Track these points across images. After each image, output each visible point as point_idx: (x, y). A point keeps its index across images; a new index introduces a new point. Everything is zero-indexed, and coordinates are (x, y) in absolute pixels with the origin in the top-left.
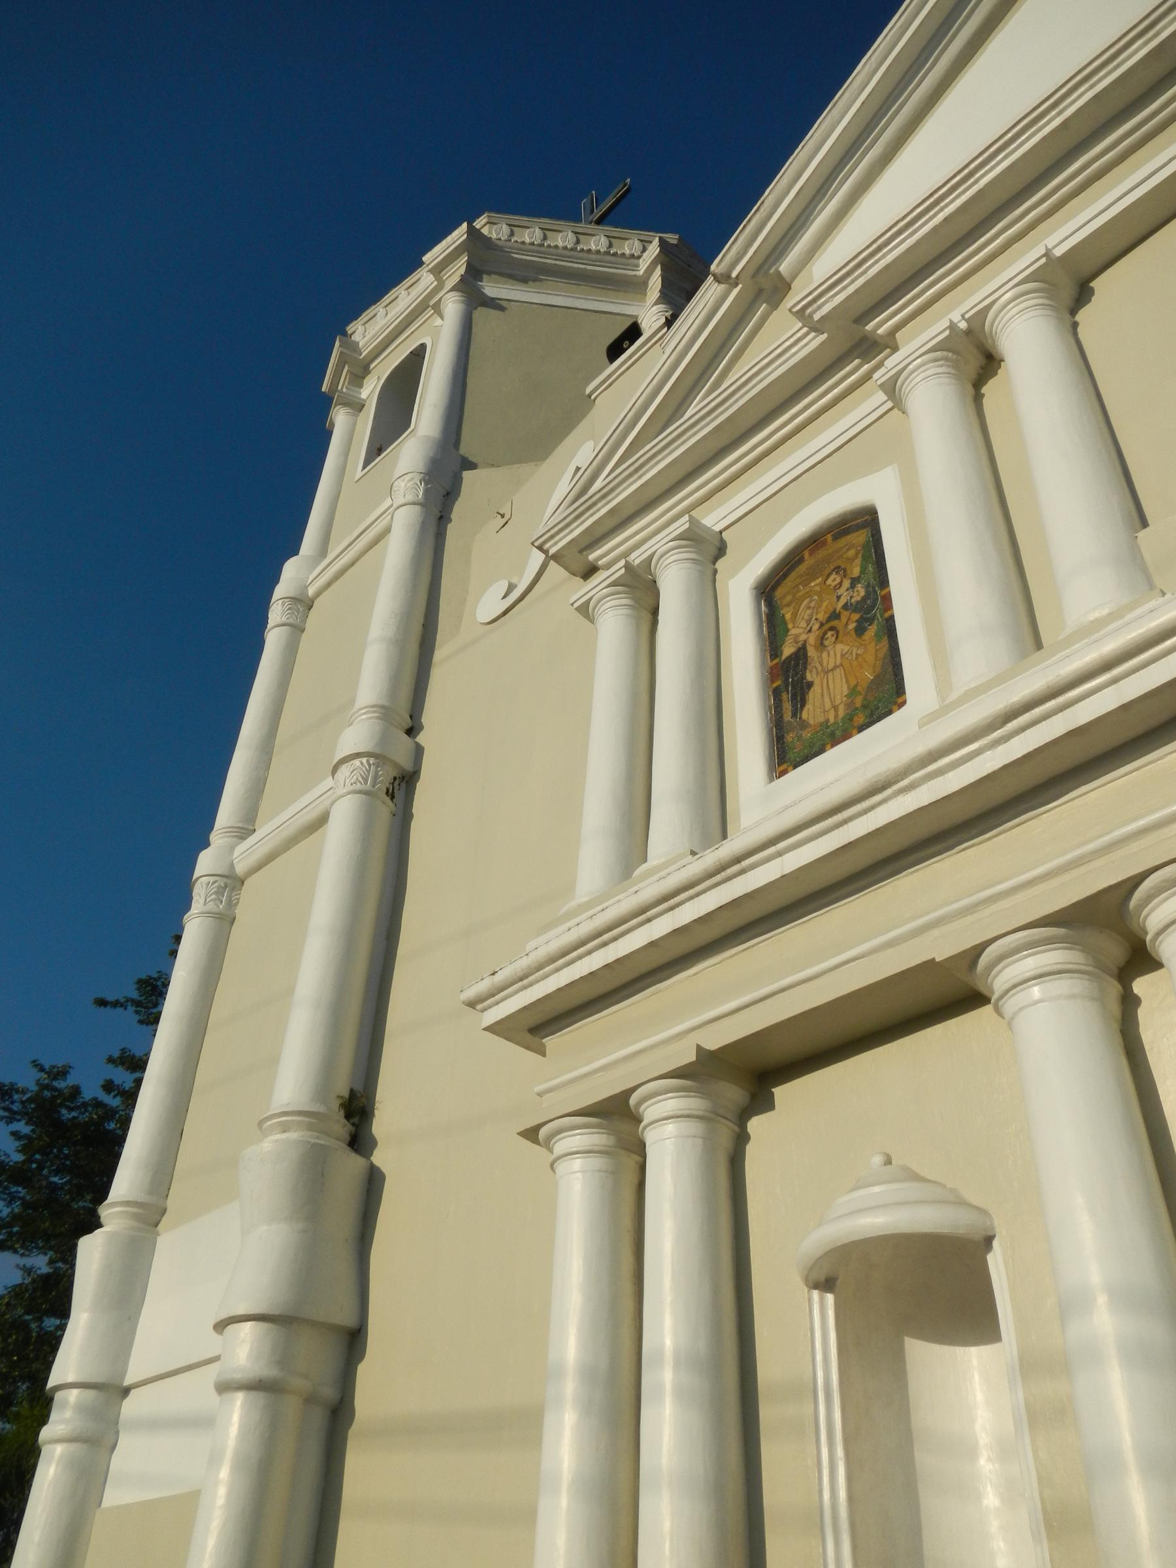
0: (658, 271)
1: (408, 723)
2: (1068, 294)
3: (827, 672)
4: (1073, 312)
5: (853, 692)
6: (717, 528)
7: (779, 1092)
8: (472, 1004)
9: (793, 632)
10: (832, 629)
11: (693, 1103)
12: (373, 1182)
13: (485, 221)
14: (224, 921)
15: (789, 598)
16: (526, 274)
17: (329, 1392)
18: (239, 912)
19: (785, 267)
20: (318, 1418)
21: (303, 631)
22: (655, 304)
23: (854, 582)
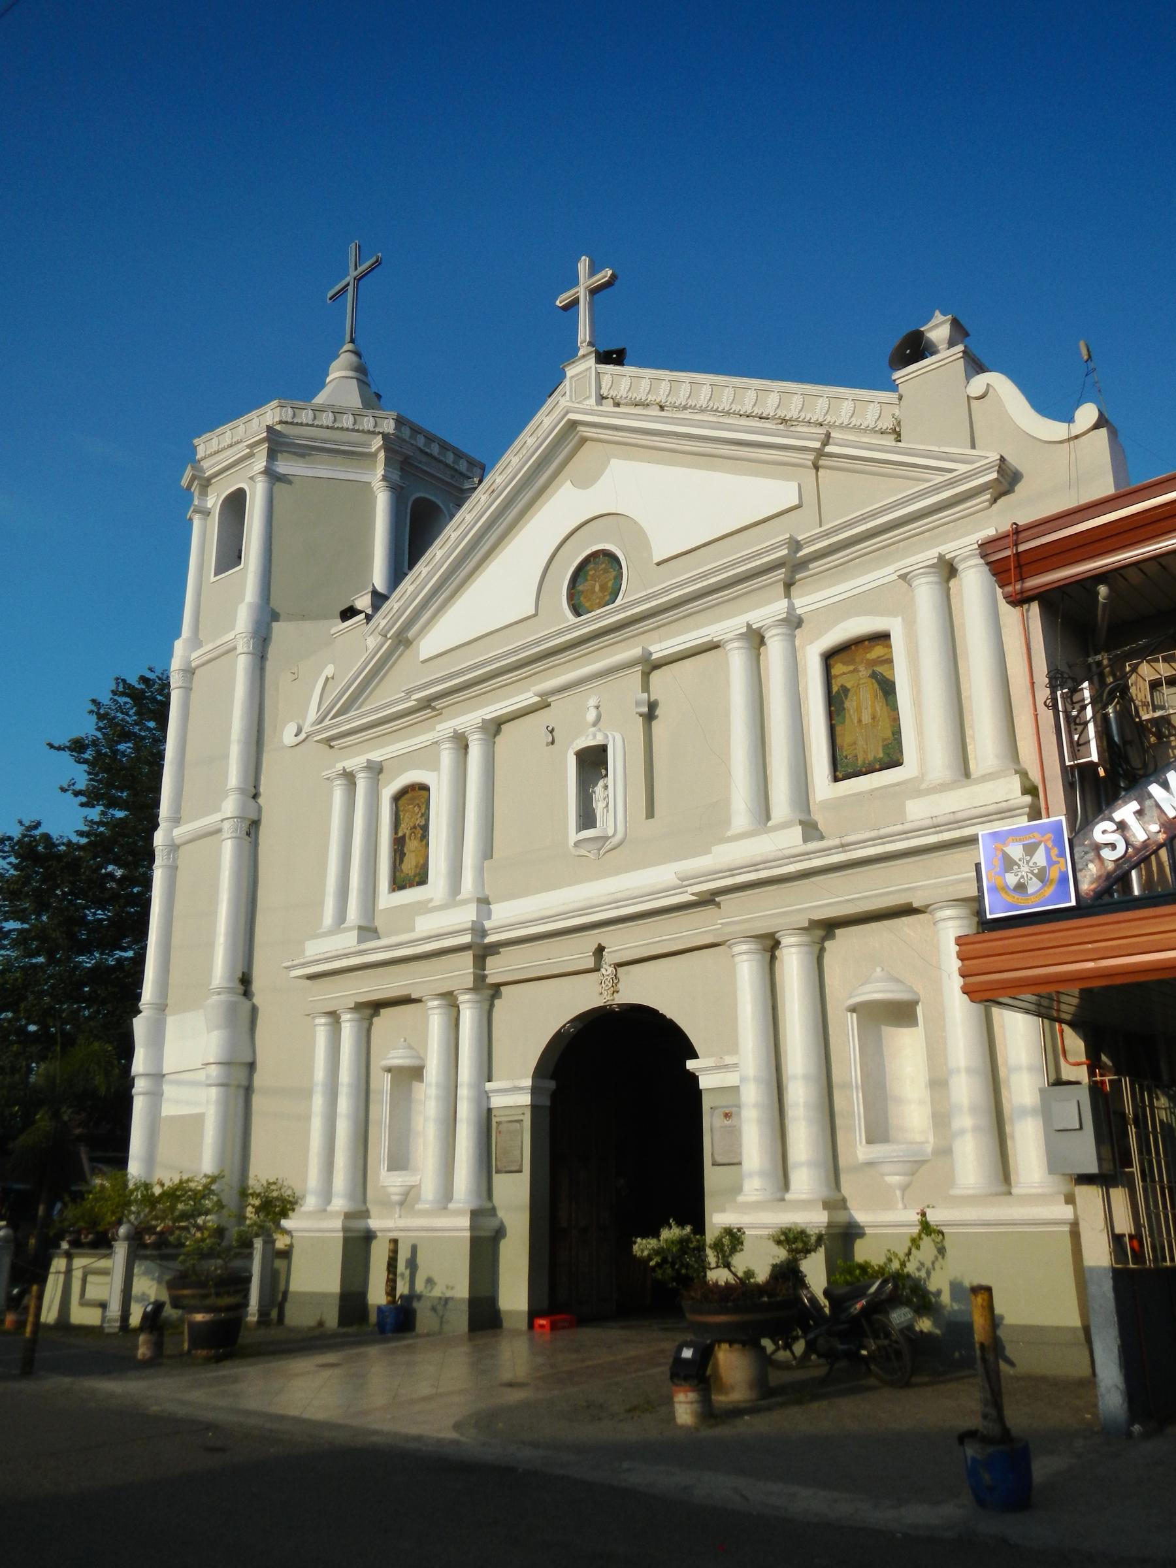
0: (382, 454)
1: (253, 791)
2: (493, 731)
3: (410, 851)
4: (495, 736)
5: (416, 866)
6: (379, 759)
7: (383, 1011)
8: (287, 968)
9: (402, 825)
10: (414, 832)
11: (355, 1016)
12: (254, 1010)
13: (277, 405)
14: (173, 869)
15: (402, 808)
16: (303, 452)
17: (244, 1083)
18: (179, 863)
19: (410, 635)
20: (242, 1092)
21: (191, 689)
22: (381, 481)
23: (423, 815)
